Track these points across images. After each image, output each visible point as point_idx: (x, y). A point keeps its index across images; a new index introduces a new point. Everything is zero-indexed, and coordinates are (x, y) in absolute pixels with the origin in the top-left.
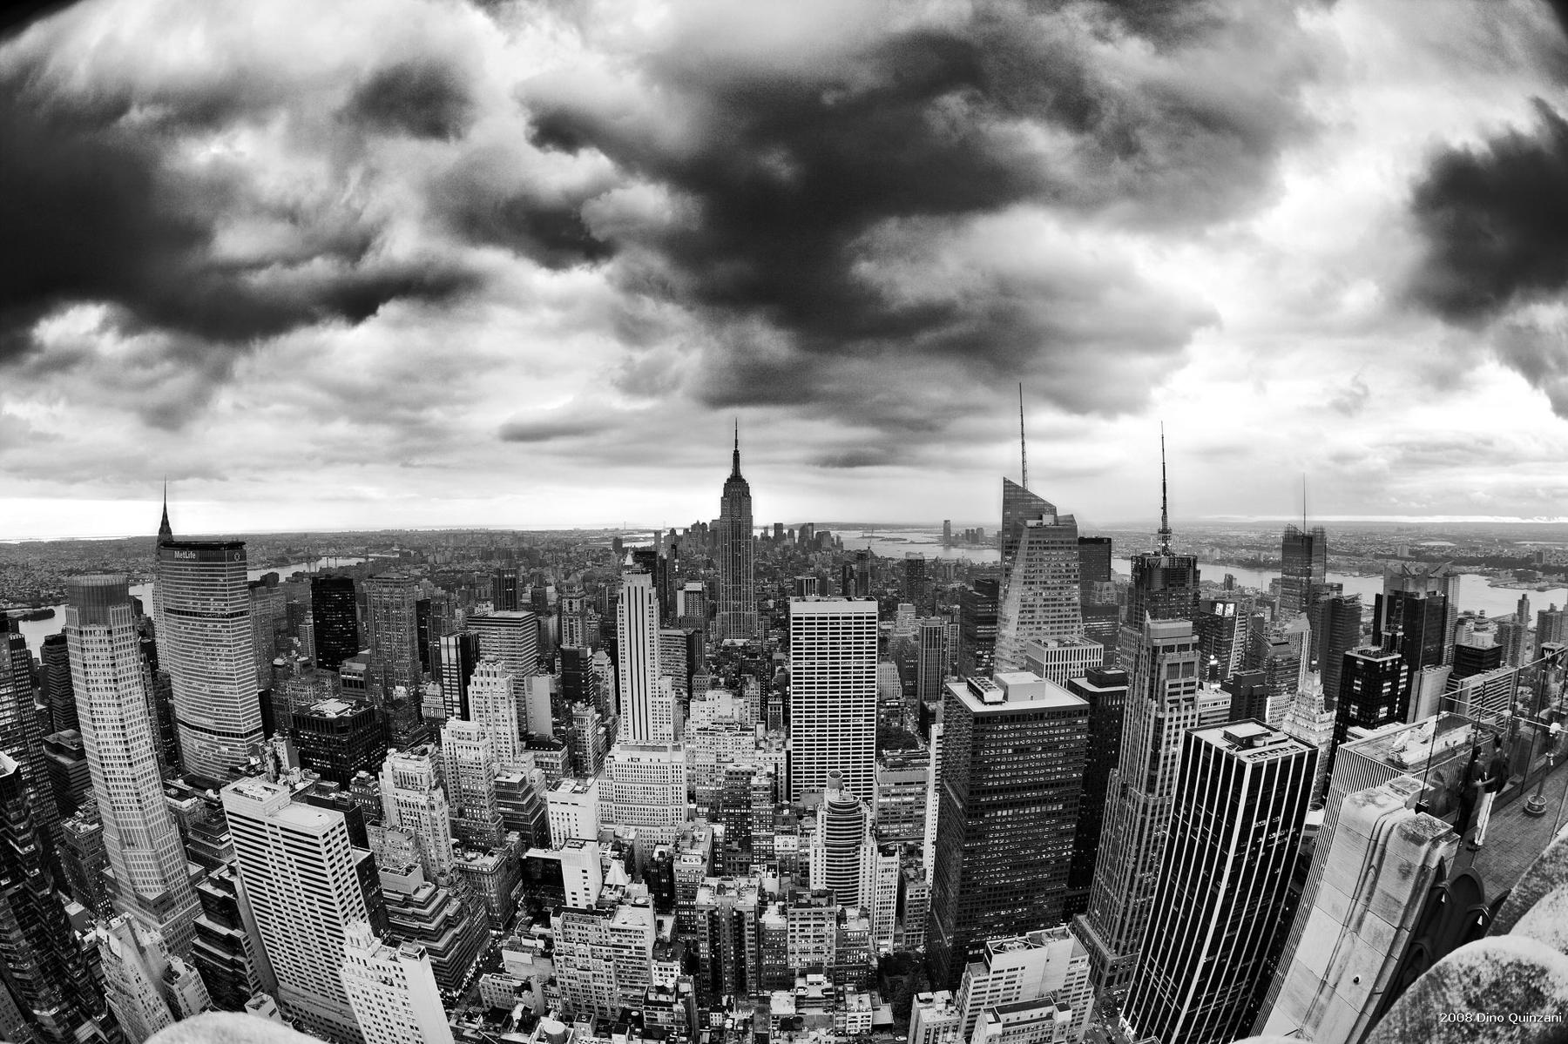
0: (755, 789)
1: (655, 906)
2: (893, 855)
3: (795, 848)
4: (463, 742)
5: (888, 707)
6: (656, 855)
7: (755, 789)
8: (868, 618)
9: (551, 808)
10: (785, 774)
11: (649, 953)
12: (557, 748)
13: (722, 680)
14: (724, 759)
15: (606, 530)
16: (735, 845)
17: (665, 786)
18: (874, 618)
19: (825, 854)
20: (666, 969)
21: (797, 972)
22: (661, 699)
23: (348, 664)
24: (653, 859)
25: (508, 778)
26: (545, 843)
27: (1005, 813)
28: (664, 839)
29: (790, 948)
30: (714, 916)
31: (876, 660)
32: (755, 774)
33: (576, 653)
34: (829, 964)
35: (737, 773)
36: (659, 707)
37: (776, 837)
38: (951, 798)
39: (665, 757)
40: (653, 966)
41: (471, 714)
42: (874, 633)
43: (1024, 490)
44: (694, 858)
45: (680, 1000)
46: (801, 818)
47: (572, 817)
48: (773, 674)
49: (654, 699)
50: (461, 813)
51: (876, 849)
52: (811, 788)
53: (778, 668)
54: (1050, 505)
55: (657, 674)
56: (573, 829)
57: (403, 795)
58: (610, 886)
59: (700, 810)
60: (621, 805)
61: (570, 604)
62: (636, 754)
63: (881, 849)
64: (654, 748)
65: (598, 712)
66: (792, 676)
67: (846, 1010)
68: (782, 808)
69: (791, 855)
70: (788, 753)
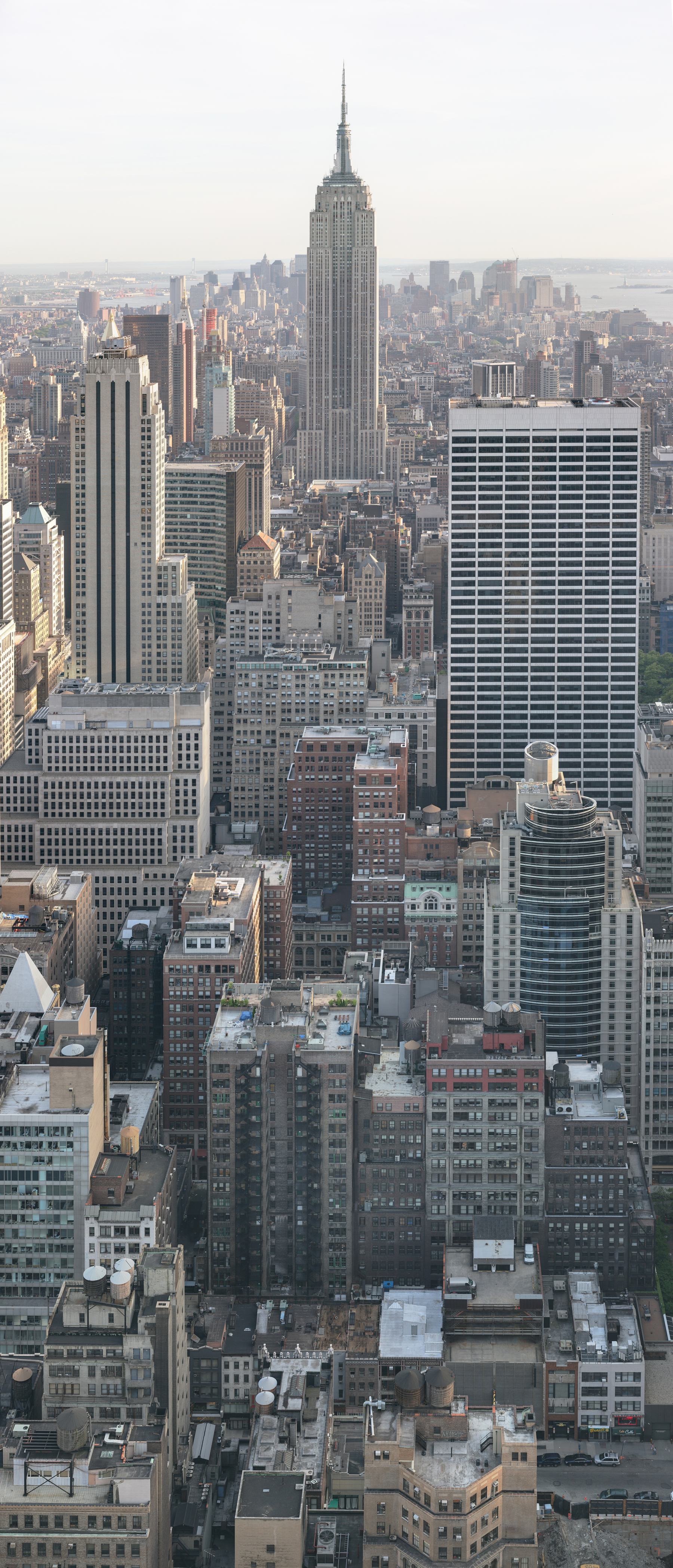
1: (111, 1058)
7: (363, 781)
11: (85, 1190)
16: (313, 907)
20: (120, 1231)
21: (449, 1233)
29: (431, 1161)
30: (250, 1079)
32: (364, 749)
34: (529, 1210)
35: (324, 748)
40: (88, 1225)
45: (142, 1321)
46: (464, 843)
62: (97, 713)
67: (572, 1352)
70: (441, 705)
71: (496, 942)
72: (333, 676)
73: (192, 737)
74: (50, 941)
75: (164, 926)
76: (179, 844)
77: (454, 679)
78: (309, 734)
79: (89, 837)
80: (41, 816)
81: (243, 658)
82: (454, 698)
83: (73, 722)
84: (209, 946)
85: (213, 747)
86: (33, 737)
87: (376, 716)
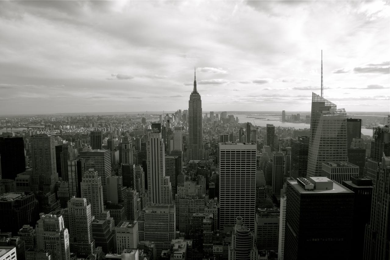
0: (205, 225)
2: (265, 256)
3: (222, 251)
4: (79, 207)
5: (260, 190)
6: (162, 254)
7: (205, 225)
8: (252, 152)
9: (118, 235)
10: (217, 218)
12: (120, 208)
13: (190, 177)
14: (191, 211)
15: (138, 115)
17: (167, 223)
18: (255, 152)
19: (235, 254)
22: (165, 186)
23: (20, 176)
24: (161, 256)
25: (98, 222)
26: (114, 252)
27: (316, 240)
28: (166, 247)
31: (256, 170)
32: (205, 218)
33: (128, 167)
35: (197, 218)
36: (164, 189)
37: (213, 246)
38: (291, 232)
39: (167, 211)
41: (82, 195)
42: (255, 158)
43: (322, 98)
44: (179, 255)
46: (224, 237)
47: (127, 239)
48: (211, 175)
50: (75, 240)
51: (257, 253)
52: (228, 224)
53: (213, 172)
54: (334, 104)
55: (164, 175)
56: (127, 243)
57: (48, 234)
59: (181, 233)
60: (147, 233)
61: (126, 146)
62: (155, 210)
63: (259, 253)
64: (162, 207)
65: (137, 192)
66: (220, 176)
68: (216, 233)
69: (220, 255)
70: (218, 209)
71: (231, 257)
72: (198, 202)
73: (173, 215)
74: (149, 255)
75: (169, 253)
76: (171, 237)
77: (221, 203)
78: (194, 215)
79: (154, 235)
80: (145, 230)
81: (181, 199)
82: (221, 207)
83: (150, 211)
84: (178, 257)
85: (176, 217)
86: (143, 214)
87: (206, 211)
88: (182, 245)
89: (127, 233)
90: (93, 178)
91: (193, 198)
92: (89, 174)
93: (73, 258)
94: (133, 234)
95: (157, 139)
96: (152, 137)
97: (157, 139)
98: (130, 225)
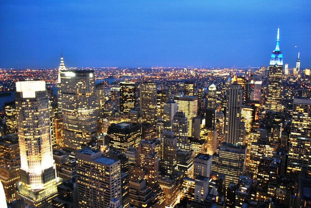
6: (230, 186)
10: (284, 164)
13: (265, 125)
22: (240, 130)
49: (237, 129)
58: (211, 195)
62: (228, 148)
88: (248, 182)
89: (203, 164)
90: (182, 117)
91: (263, 143)
92: (178, 114)
93: (161, 176)
94: (207, 165)
95: (236, 90)
96: (232, 88)
97: (236, 90)
98: (205, 158)
